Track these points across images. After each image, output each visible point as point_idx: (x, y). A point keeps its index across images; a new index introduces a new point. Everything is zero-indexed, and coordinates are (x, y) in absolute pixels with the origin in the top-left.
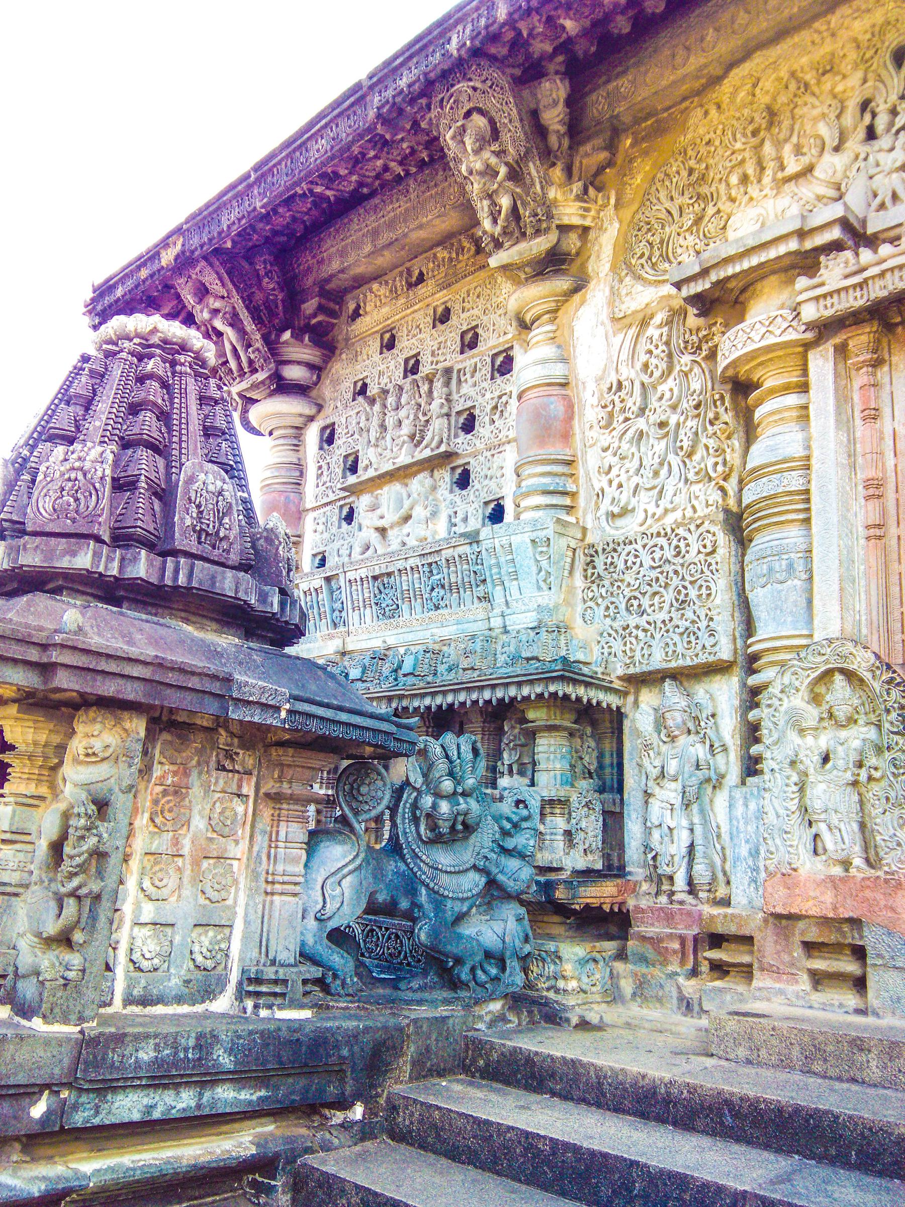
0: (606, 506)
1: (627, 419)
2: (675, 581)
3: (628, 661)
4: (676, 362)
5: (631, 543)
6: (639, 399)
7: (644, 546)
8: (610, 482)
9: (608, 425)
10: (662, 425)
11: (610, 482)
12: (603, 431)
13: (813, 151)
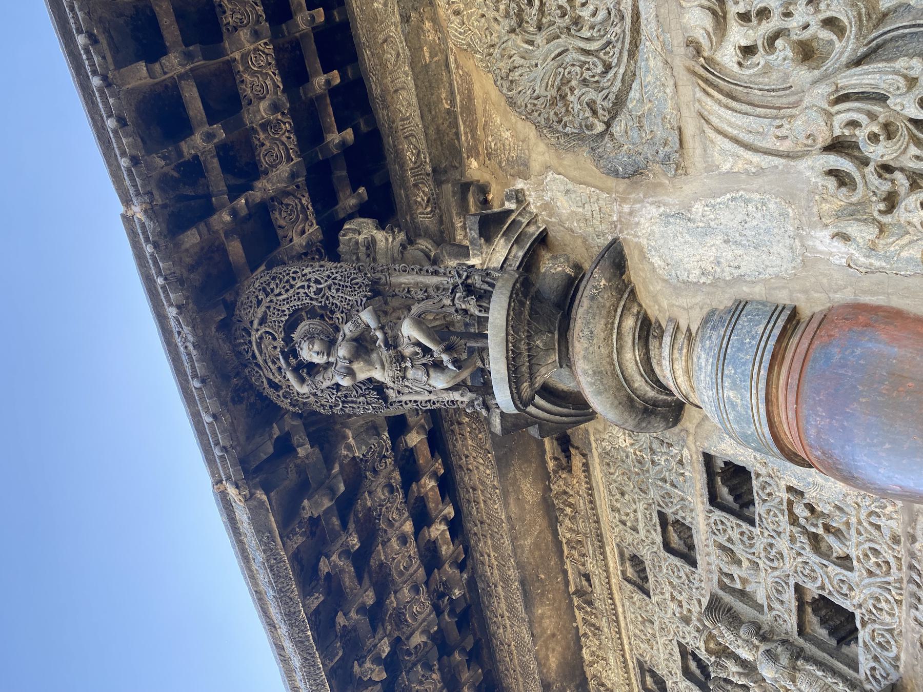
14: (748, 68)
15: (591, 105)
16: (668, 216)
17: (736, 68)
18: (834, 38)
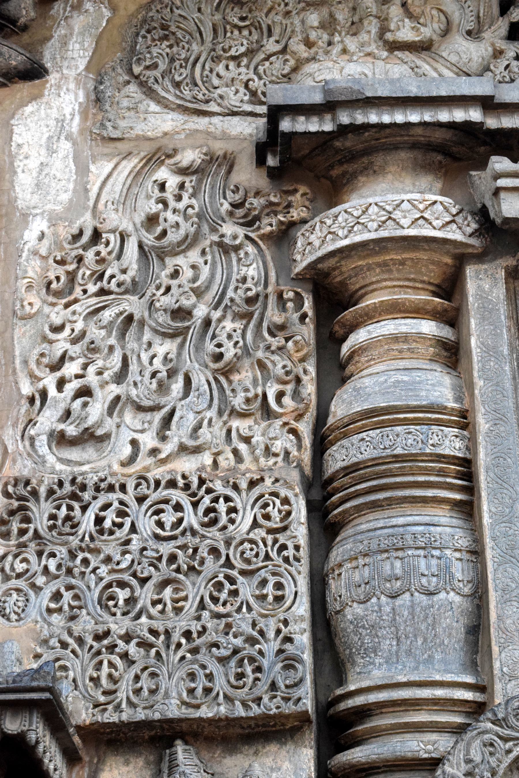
0: (48, 420)
1: (102, 292)
2: (211, 566)
3: (102, 699)
4: (205, 228)
5: (111, 488)
6: (135, 266)
7: (141, 500)
8: (61, 384)
9: (61, 291)
10: (181, 313)
11: (61, 384)
12: (51, 299)
13: (436, 26)
14: (153, 186)
15: (155, 66)
16: (63, 121)
17: (154, 178)
18: (156, 235)
